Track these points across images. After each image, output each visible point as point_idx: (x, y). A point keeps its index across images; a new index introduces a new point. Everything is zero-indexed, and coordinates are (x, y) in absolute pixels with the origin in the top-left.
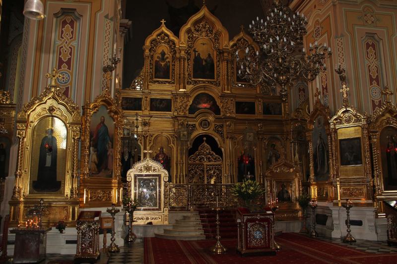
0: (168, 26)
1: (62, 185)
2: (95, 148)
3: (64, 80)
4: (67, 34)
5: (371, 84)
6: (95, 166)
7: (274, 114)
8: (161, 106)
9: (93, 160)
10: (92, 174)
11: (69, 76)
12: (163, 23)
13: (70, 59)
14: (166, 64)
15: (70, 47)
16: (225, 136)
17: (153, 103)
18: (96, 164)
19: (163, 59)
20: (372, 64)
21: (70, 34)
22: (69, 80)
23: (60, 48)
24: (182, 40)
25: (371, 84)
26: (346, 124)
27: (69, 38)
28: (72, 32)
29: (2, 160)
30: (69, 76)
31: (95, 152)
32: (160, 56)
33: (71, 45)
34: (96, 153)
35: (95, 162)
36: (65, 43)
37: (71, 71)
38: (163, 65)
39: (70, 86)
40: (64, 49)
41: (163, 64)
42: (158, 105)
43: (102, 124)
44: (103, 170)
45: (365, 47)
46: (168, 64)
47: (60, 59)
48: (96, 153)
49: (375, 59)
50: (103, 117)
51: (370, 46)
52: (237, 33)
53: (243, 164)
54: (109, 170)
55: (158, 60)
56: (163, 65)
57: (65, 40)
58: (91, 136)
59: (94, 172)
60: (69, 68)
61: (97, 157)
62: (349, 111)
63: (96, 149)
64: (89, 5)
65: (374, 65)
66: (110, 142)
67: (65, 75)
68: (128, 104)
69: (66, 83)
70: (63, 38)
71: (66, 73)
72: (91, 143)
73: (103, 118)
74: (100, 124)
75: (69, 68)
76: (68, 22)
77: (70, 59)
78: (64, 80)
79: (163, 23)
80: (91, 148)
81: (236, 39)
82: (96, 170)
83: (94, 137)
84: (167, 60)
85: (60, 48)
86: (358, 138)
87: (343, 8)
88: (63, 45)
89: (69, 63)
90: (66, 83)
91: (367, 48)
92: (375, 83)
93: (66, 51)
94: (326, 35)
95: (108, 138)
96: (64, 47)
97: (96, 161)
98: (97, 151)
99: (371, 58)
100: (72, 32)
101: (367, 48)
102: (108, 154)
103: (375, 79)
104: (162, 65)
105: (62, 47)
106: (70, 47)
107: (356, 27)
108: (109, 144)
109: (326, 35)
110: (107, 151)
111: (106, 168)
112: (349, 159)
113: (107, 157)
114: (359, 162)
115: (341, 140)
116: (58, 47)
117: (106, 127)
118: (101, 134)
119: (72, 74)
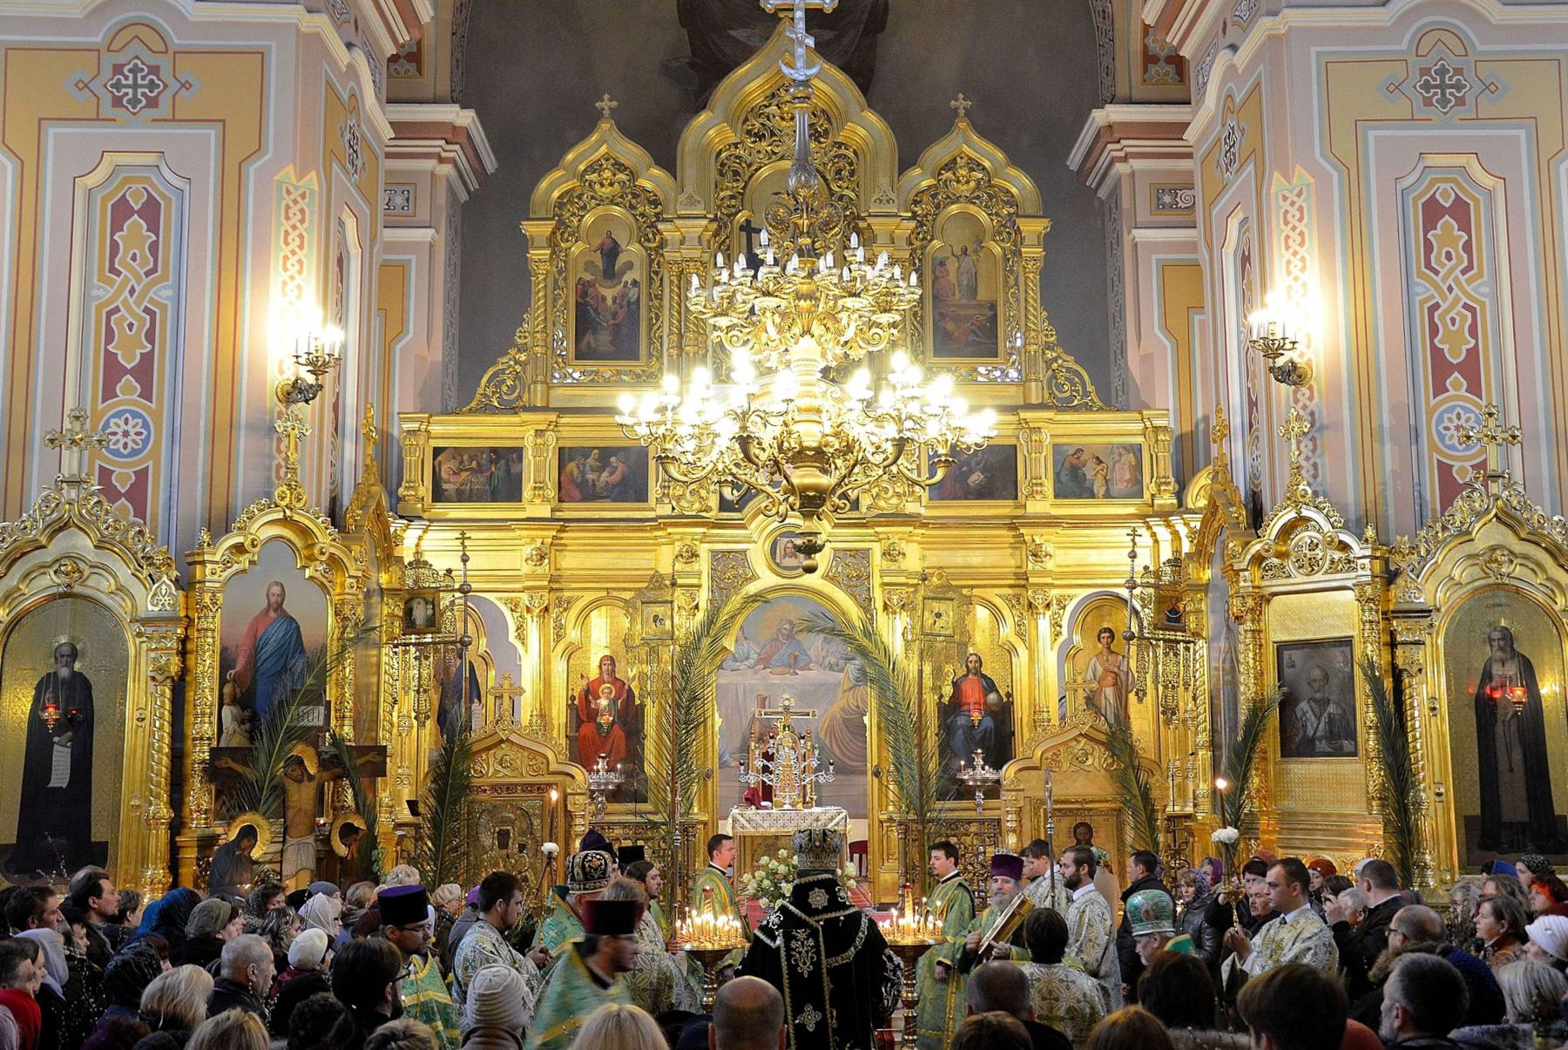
0: (629, 130)
1: (110, 852)
3: (128, 440)
4: (134, 258)
5: (1440, 388)
7: (1108, 495)
8: (605, 474)
11: (146, 425)
12: (606, 113)
13: (147, 358)
14: (624, 295)
15: (147, 310)
16: (878, 597)
17: (571, 466)
19: (610, 273)
20: (1451, 297)
21: (143, 257)
22: (146, 442)
23: (110, 314)
24: (689, 189)
25: (1440, 388)
26: (1301, 578)
27: (142, 272)
28: (154, 248)
30: (146, 425)
31: (242, 722)
32: (598, 259)
33: (152, 301)
36: (126, 293)
38: (609, 302)
40: (124, 318)
41: (609, 293)
42: (590, 476)
43: (272, 614)
45: (1416, 217)
46: (633, 293)
47: (110, 358)
49: (1464, 272)
50: (277, 583)
51: (1443, 211)
52: (944, 126)
53: (961, 720)
55: (588, 277)
56: (609, 302)
57: (127, 280)
58: (226, 664)
60: (146, 394)
62: (1309, 519)
64: (212, 133)
65: (1457, 300)
67: (131, 423)
68: (464, 475)
69: (134, 453)
70: (118, 273)
71: (136, 415)
72: (227, 689)
73: (276, 590)
74: (267, 611)
75: (146, 394)
76: (136, 208)
77: (147, 358)
78: (128, 440)
79: (606, 113)
81: (939, 152)
83: (239, 667)
84: (629, 277)
85: (154, 270)
86: (1347, 642)
87: (1314, 50)
88: (118, 303)
89: (144, 372)
90: (134, 453)
91: (1430, 223)
92: (1457, 387)
93: (131, 326)
94: (1250, 168)
96: (123, 311)
99: (1443, 272)
100: (154, 248)
101: (1430, 223)
103: (1460, 368)
104: (604, 299)
105: (117, 310)
106: (147, 310)
107: (1372, 134)
109: (1250, 168)
112: (1310, 732)
114: (1347, 745)
115: (1282, 647)
116: (99, 309)
117: (293, 619)
118: (269, 649)
119: (157, 415)
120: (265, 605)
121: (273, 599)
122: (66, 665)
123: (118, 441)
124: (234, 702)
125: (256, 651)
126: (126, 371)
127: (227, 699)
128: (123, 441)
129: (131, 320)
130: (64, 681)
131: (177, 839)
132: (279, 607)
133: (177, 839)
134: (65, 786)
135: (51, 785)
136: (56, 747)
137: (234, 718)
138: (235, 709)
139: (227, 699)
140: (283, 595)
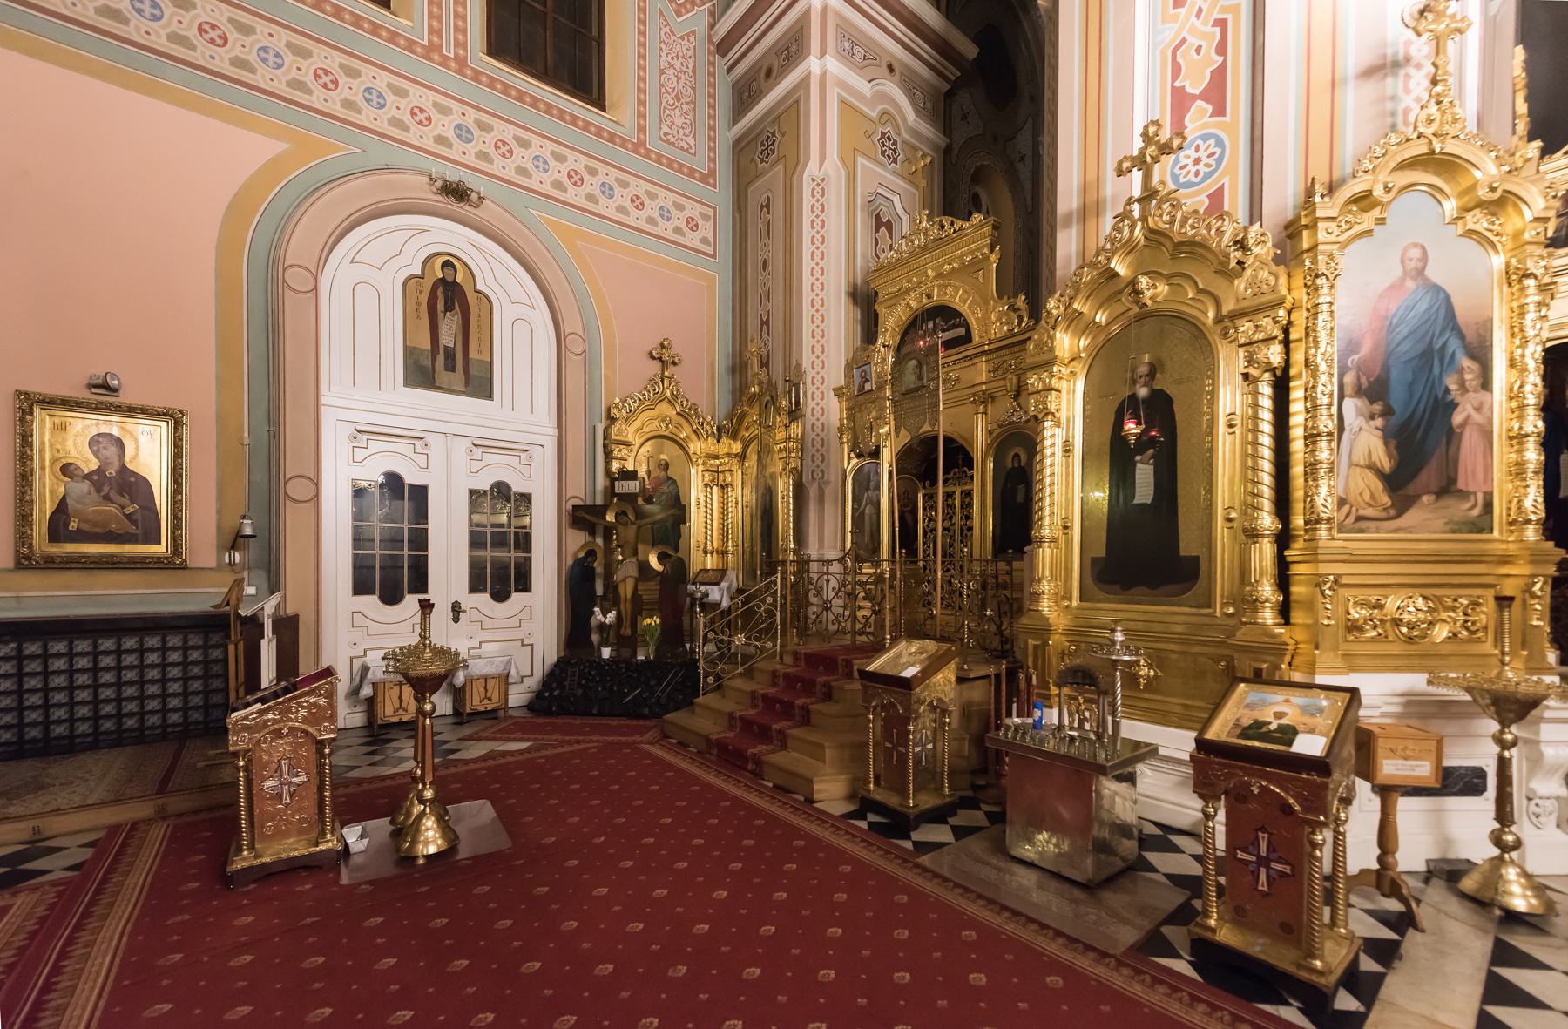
3: (1201, 167)
6: (1377, 485)
9: (1360, 457)
10: (1359, 519)
18: (1379, 473)
29: (1020, 498)
30: (1220, 143)
34: (1379, 422)
35: (1372, 467)
37: (1227, 119)
39: (1226, 180)
43: (1410, 284)
44: (1425, 499)
50: (1416, 245)
54: (1464, 495)
59: (1370, 512)
63: (1377, 407)
66: (1466, 363)
72: (1349, 379)
73: (1415, 253)
74: (1403, 279)
80: (1350, 405)
82: (1385, 500)
95: (1454, 345)
98: (1387, 412)
102: (1457, 418)
108: (1461, 371)
110: (1453, 406)
111: (1448, 488)
113: (1452, 436)
117: (1437, 289)
120: (1398, 272)
121: (1411, 265)
122: (1145, 385)
123: (1189, 172)
124: (1359, 392)
126: (1194, 98)
127: (1348, 390)
128: (1193, 169)
129: (1198, 43)
130: (1144, 401)
131: (1286, 553)
133: (1286, 553)
134: (1149, 502)
135: (1135, 502)
136: (1139, 466)
137: (1359, 413)
138: (1360, 403)
139: (1348, 390)
140: (1424, 258)
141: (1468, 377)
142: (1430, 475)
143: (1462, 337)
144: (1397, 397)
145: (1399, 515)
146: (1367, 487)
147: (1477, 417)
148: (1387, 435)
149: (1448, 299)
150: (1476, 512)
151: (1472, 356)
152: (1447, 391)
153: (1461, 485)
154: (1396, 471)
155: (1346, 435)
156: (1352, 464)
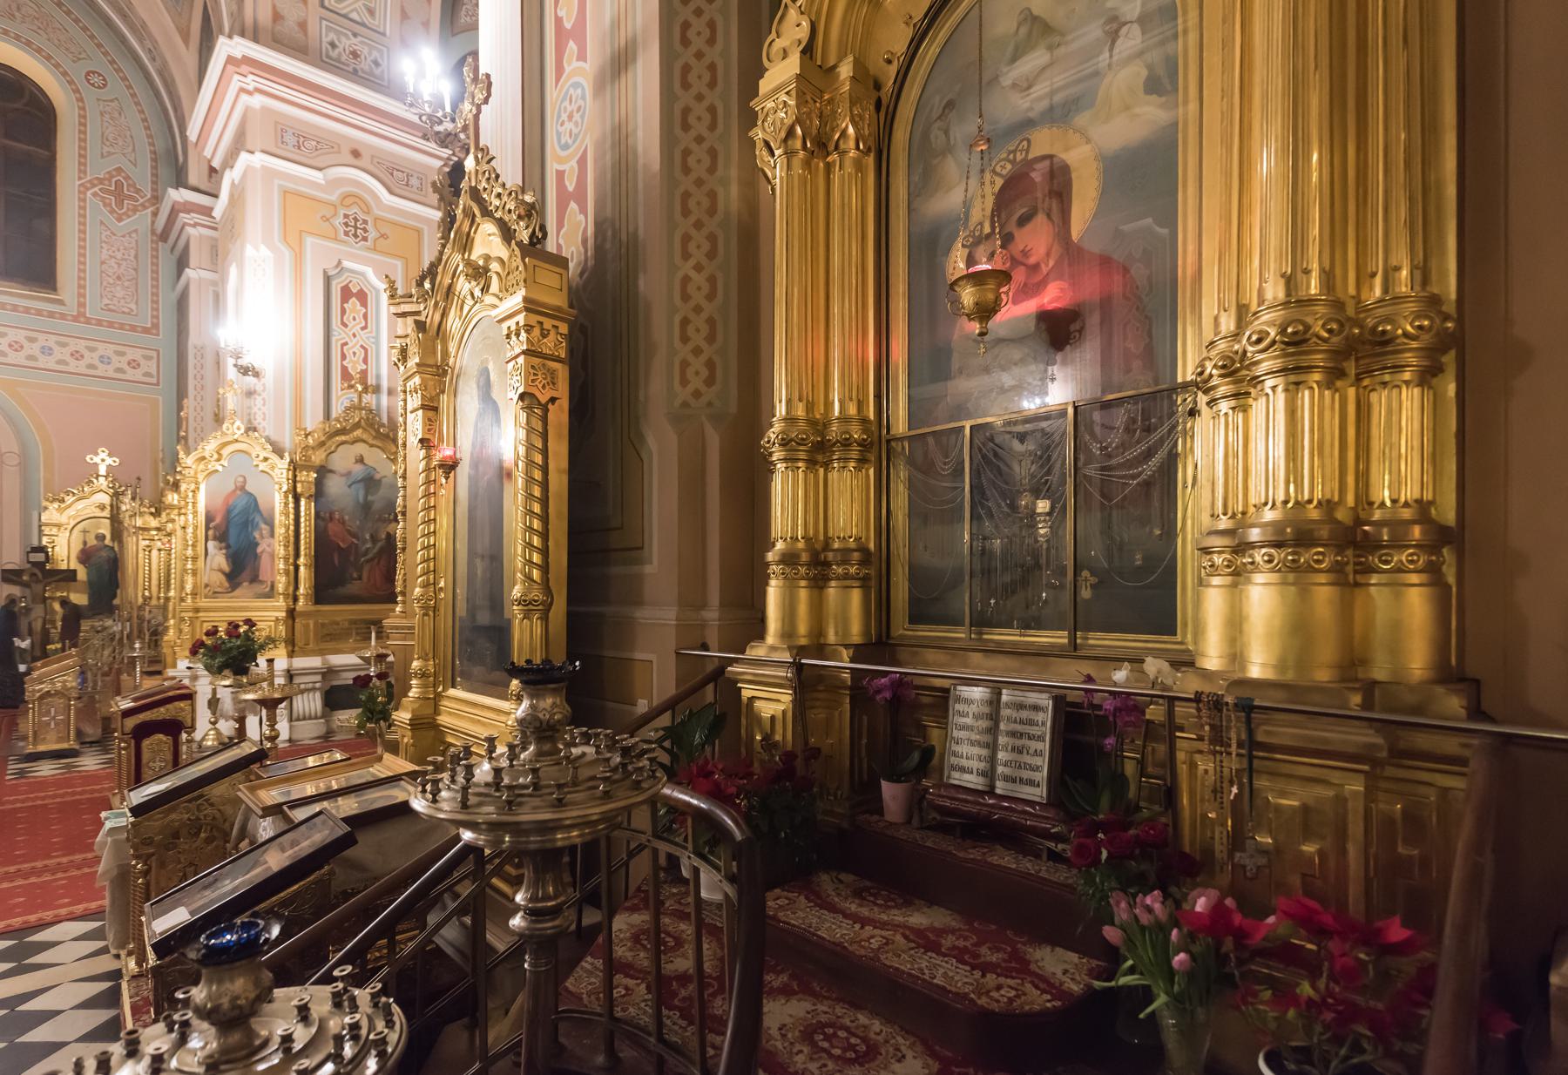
2: (221, 542)
9: (215, 566)
34: (224, 551)
43: (238, 492)
44: (245, 584)
48: (224, 551)
54: (261, 582)
61: (227, 558)
63: (223, 545)
72: (211, 533)
73: (241, 479)
74: (234, 491)
80: (211, 544)
82: (227, 585)
83: (218, 520)
95: (258, 518)
97: (227, 569)
98: (228, 547)
102: (259, 550)
108: (261, 530)
111: (255, 579)
113: (256, 557)
117: (252, 494)
118: (236, 511)
120: (233, 487)
121: (238, 484)
124: (215, 538)
125: (229, 512)
132: (242, 488)
137: (215, 547)
138: (216, 543)
140: (245, 482)
141: (264, 532)
142: (246, 574)
143: (262, 515)
144: (232, 540)
145: (233, 591)
146: (218, 579)
147: (268, 549)
148: (227, 557)
149: (255, 500)
150: (268, 589)
151: (266, 523)
152: (255, 538)
153: (260, 578)
154: (232, 571)
155: (209, 557)
156: (212, 569)
